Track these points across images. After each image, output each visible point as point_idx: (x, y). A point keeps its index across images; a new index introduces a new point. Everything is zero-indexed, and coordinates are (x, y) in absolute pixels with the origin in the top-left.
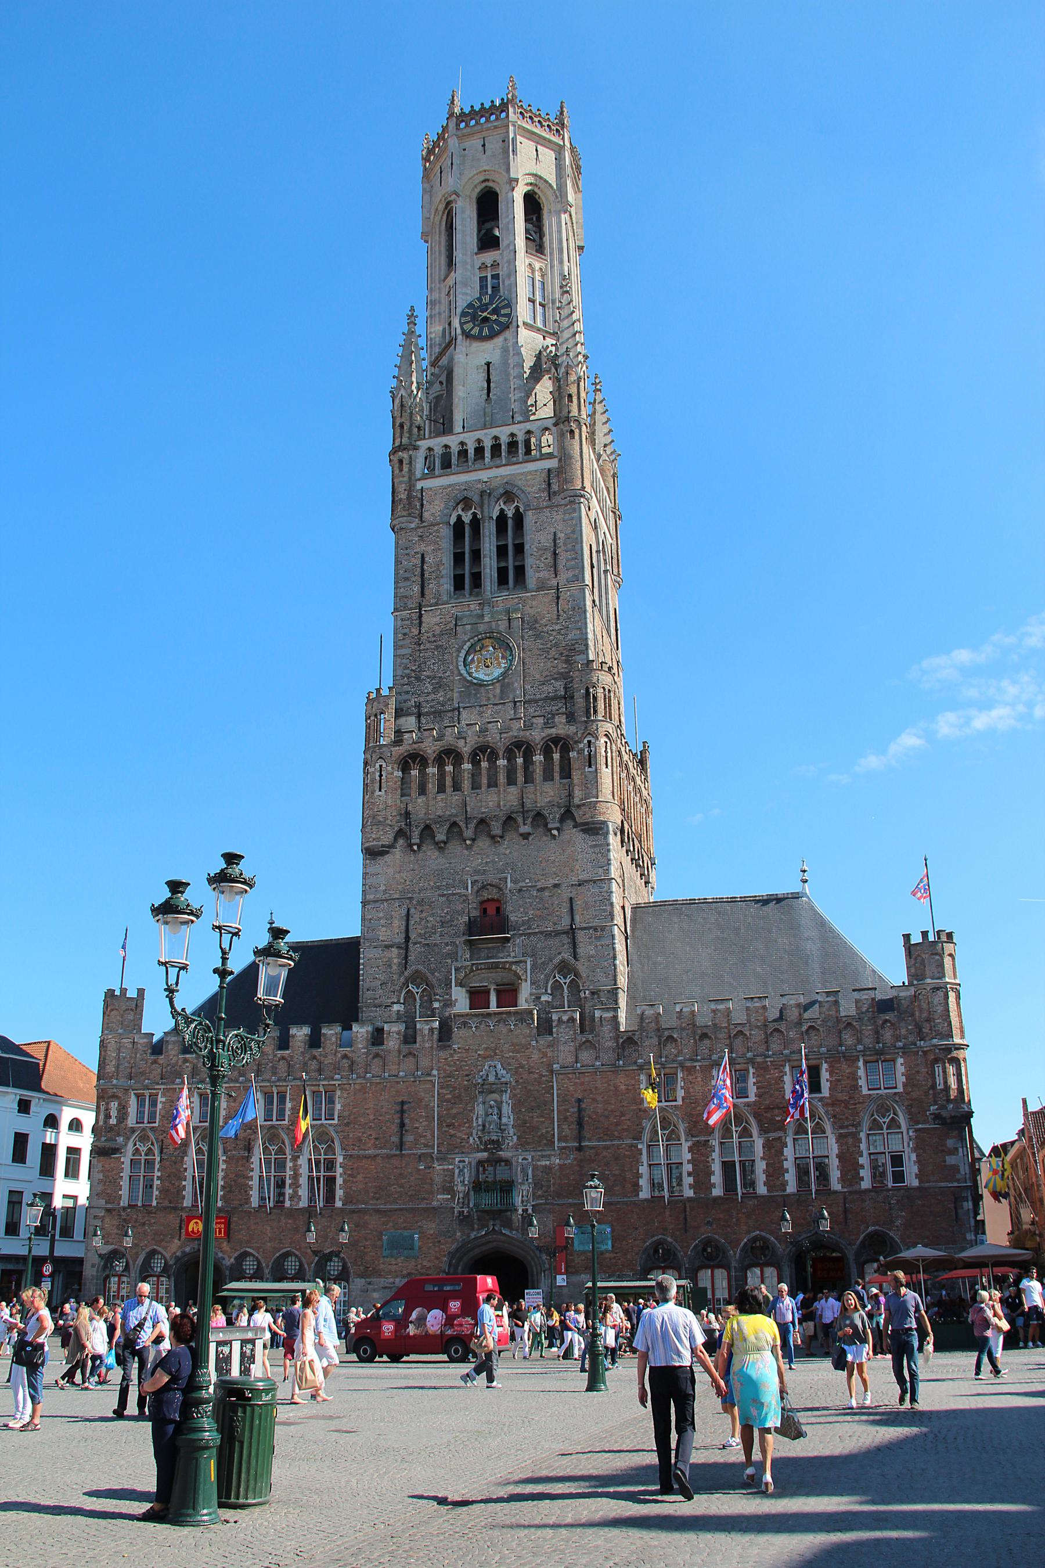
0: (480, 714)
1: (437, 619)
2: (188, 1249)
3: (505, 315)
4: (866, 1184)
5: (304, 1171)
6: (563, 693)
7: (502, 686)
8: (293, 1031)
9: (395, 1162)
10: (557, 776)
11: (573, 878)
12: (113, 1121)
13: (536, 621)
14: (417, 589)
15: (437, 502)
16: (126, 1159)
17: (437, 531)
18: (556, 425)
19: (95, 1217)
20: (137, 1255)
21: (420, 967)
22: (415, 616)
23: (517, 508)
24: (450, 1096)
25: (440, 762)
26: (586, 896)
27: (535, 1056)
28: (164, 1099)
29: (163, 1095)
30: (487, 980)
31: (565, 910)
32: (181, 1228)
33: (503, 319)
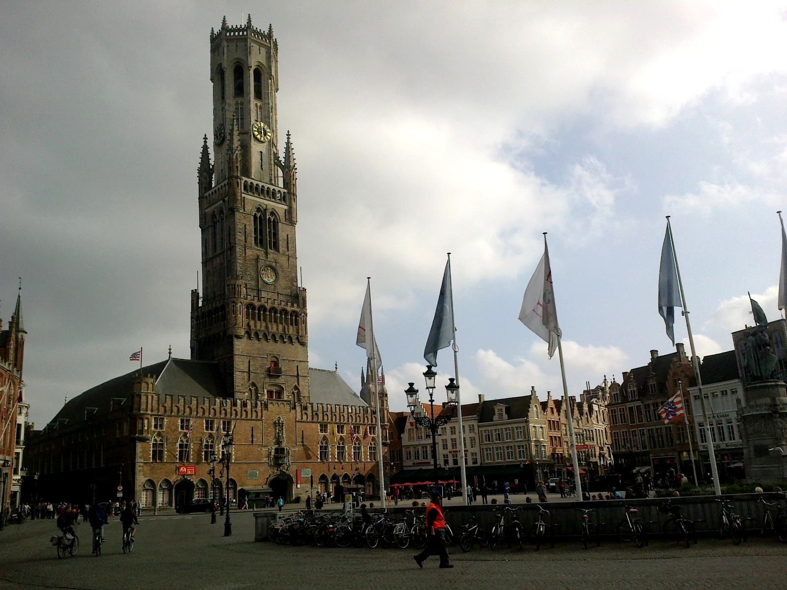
0: (268, 294)
1: (251, 253)
2: (179, 478)
3: (269, 136)
4: (369, 460)
5: (221, 449)
6: (290, 294)
7: (274, 286)
8: (217, 399)
9: (251, 447)
10: (294, 324)
11: (298, 360)
12: (146, 428)
13: (282, 266)
14: (243, 238)
15: (249, 205)
16: (151, 443)
17: (250, 217)
18: (288, 193)
19: (139, 466)
20: (159, 481)
21: (254, 381)
22: (243, 249)
23: (274, 219)
24: (266, 426)
25: (259, 310)
26: (301, 366)
27: (291, 415)
28: (166, 420)
29: (166, 419)
30: (274, 389)
31: (296, 369)
32: (176, 470)
33: (269, 138)
